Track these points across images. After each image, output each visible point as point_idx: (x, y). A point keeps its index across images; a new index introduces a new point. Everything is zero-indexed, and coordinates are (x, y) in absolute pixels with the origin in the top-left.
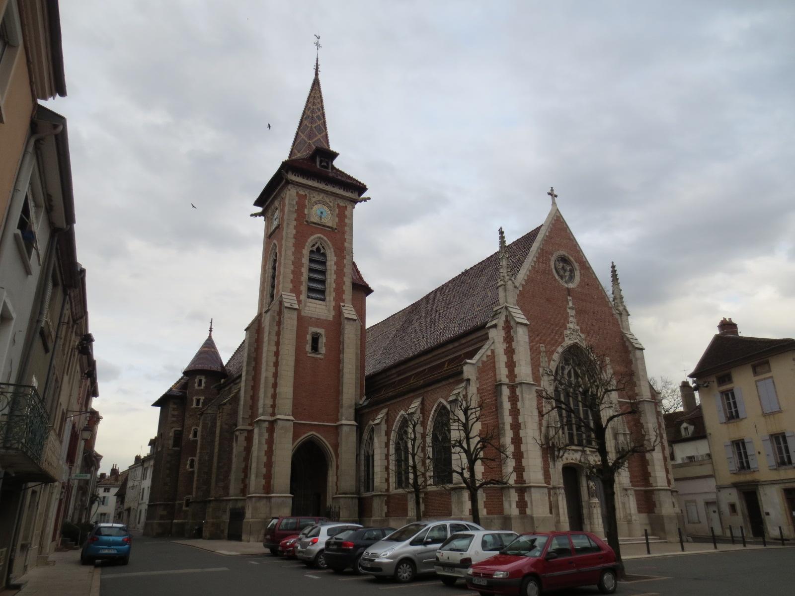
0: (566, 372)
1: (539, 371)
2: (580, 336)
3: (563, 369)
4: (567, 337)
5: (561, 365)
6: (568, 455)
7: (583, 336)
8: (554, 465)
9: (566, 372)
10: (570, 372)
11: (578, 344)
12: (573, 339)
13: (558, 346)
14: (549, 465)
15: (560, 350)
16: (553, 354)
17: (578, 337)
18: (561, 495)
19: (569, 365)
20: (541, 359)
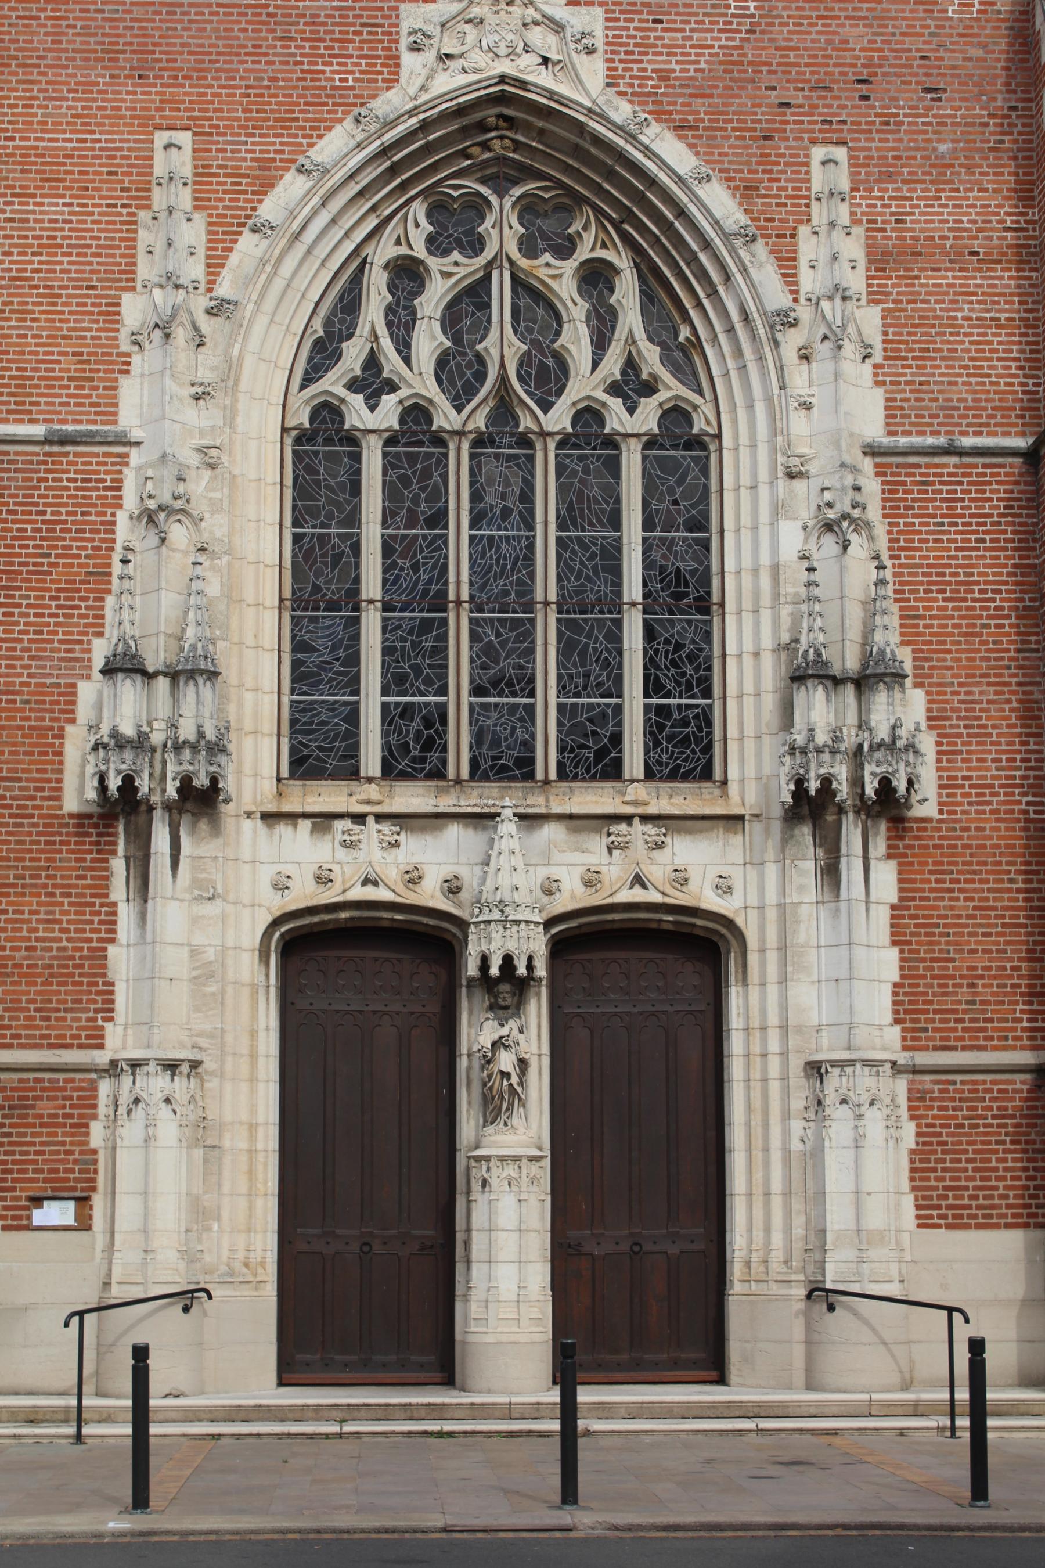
0: (433, 300)
1: (112, 313)
2: (558, 27)
3: (407, 275)
4: (416, 48)
5: (385, 251)
6: (341, 854)
7: (590, 20)
8: (143, 916)
9: (433, 300)
10: (473, 298)
11: (523, 84)
12: (479, 59)
13: (319, 130)
14: (111, 924)
15: (338, 145)
16: (267, 186)
17: (537, 36)
18: (139, 1112)
19: (475, 245)
20: (144, 237)
